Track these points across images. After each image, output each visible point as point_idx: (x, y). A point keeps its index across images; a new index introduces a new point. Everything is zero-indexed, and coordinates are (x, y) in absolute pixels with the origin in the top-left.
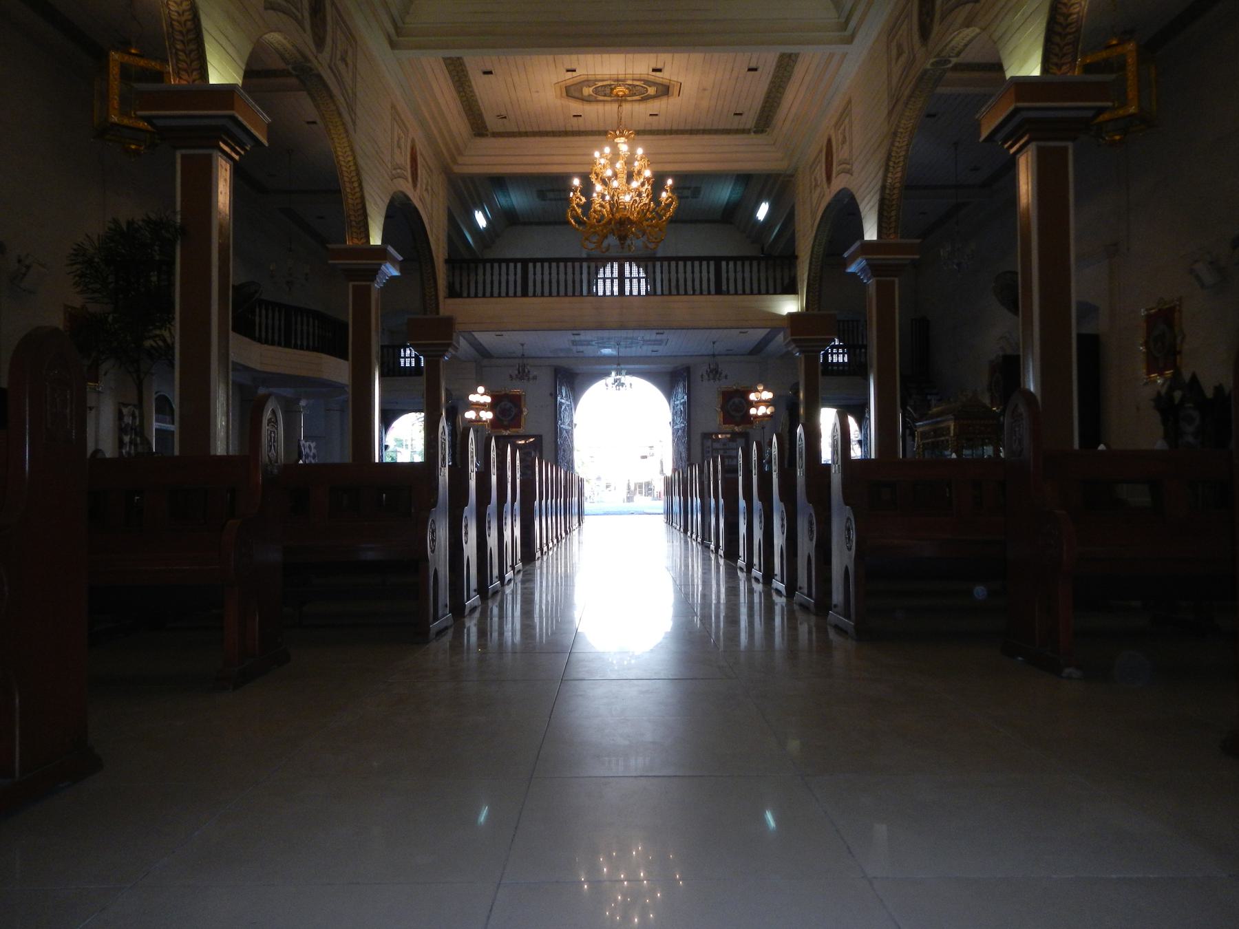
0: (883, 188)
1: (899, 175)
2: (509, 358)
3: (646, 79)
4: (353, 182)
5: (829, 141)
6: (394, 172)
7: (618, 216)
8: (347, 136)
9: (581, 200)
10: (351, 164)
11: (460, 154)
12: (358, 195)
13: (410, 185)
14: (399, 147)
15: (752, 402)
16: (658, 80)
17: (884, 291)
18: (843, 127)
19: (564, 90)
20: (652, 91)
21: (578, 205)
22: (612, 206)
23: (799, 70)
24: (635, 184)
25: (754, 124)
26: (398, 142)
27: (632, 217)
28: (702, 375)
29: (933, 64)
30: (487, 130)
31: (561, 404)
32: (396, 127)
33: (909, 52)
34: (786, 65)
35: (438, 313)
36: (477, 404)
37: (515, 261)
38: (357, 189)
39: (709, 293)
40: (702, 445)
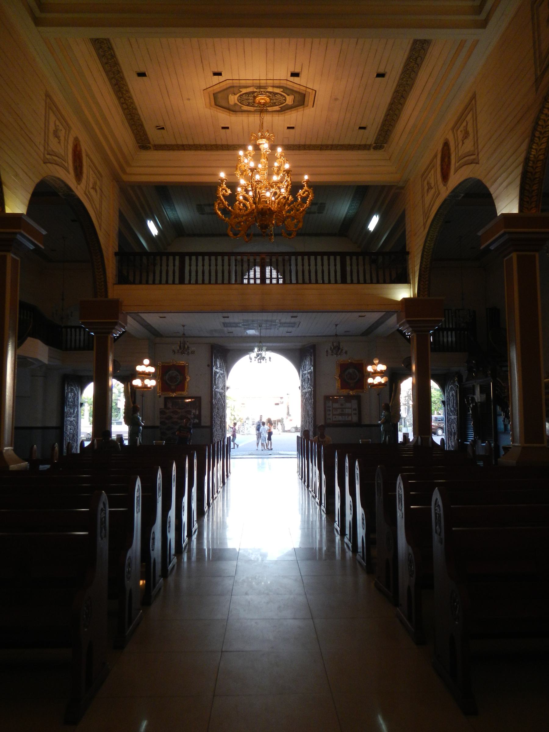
0: (527, 160)
1: (543, 146)
2: (174, 337)
3: (285, 86)
5: (446, 145)
6: (48, 157)
7: (260, 206)
9: (226, 191)
15: (370, 372)
16: (296, 88)
19: (212, 97)
25: (373, 142)
28: (327, 351)
30: (149, 143)
31: (216, 373)
35: (106, 296)
39: (336, 282)
40: (325, 404)
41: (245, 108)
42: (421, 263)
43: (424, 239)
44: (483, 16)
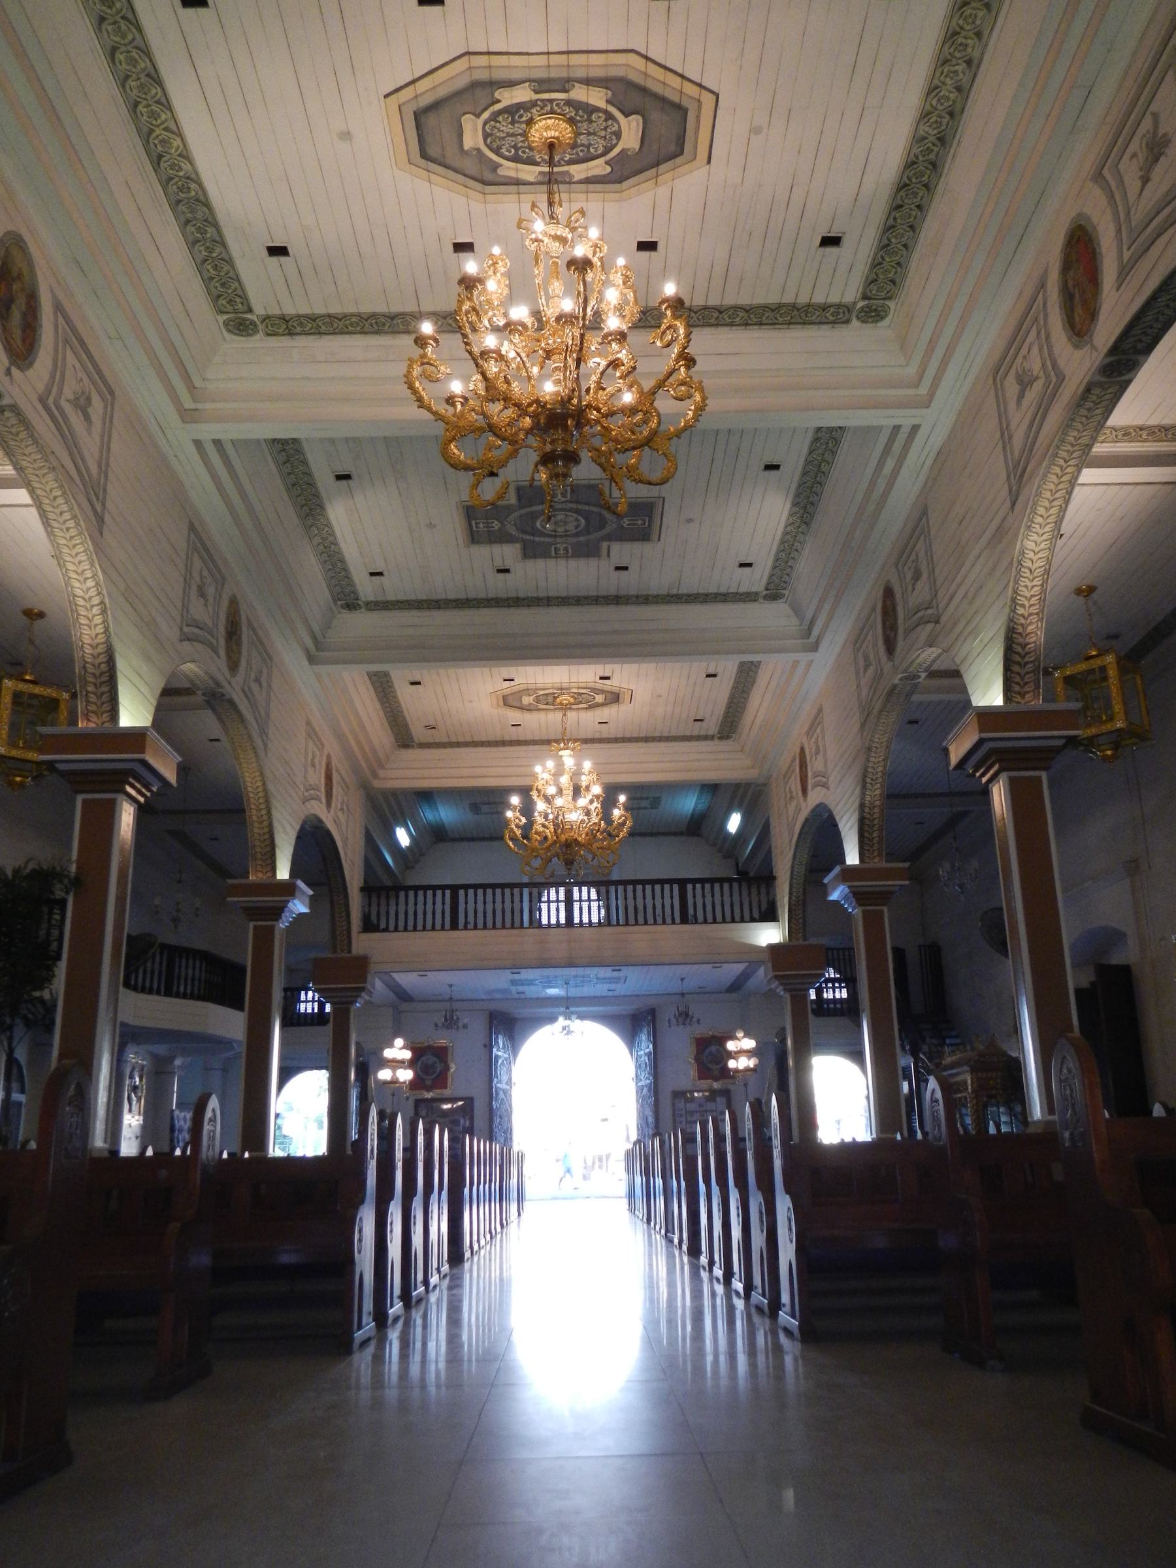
0: (862, 806)
1: (878, 792)
2: (433, 1001)
4: (260, 810)
5: (802, 749)
6: (306, 794)
7: (563, 838)
8: (258, 762)
9: (520, 820)
10: (260, 789)
11: (382, 767)
12: (266, 823)
13: (324, 806)
14: (313, 765)
17: (873, 923)
18: (815, 735)
20: (600, 699)
21: (517, 826)
22: (556, 825)
23: (763, 677)
24: (582, 802)
26: (313, 759)
27: (579, 839)
28: (669, 1020)
29: (901, 679)
31: (497, 1057)
32: (311, 744)
34: (747, 675)
35: (350, 951)
36: (394, 1061)
37: (443, 888)
38: (265, 818)
39: (673, 923)
40: (673, 1105)
42: (790, 893)
43: (790, 863)
44: (812, 639)
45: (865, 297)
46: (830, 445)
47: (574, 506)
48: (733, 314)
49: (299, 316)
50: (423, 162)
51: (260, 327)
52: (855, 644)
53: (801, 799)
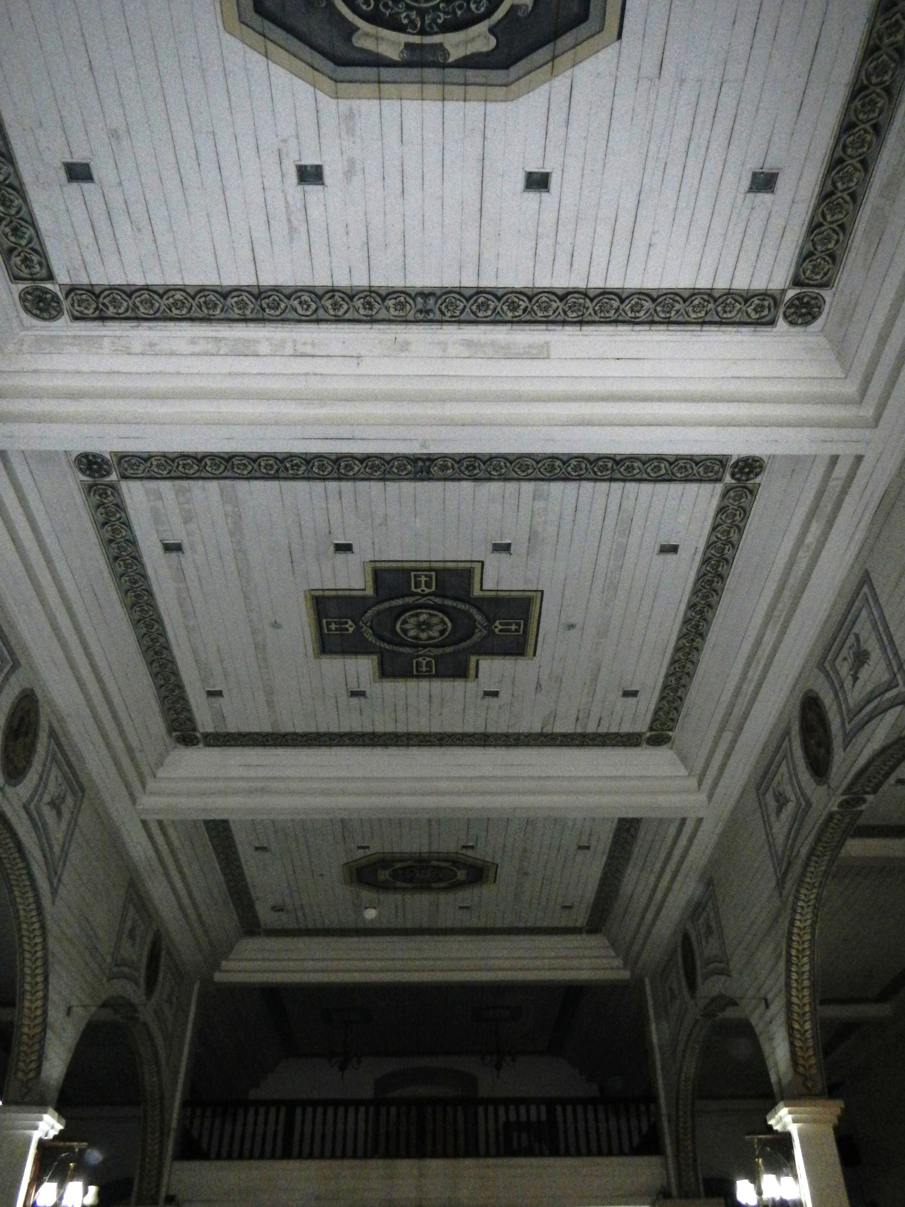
4: (36, 975)
5: (686, 938)
13: (142, 991)
18: (705, 914)
20: (461, 875)
26: (132, 930)
33: (798, 799)
37: (278, 1103)
38: (40, 986)
41: (399, 884)
45: (796, 282)
46: (738, 518)
47: (438, 601)
48: (637, 303)
49: (112, 288)
50: (257, 21)
51: (66, 304)
52: (758, 789)
53: (688, 998)
